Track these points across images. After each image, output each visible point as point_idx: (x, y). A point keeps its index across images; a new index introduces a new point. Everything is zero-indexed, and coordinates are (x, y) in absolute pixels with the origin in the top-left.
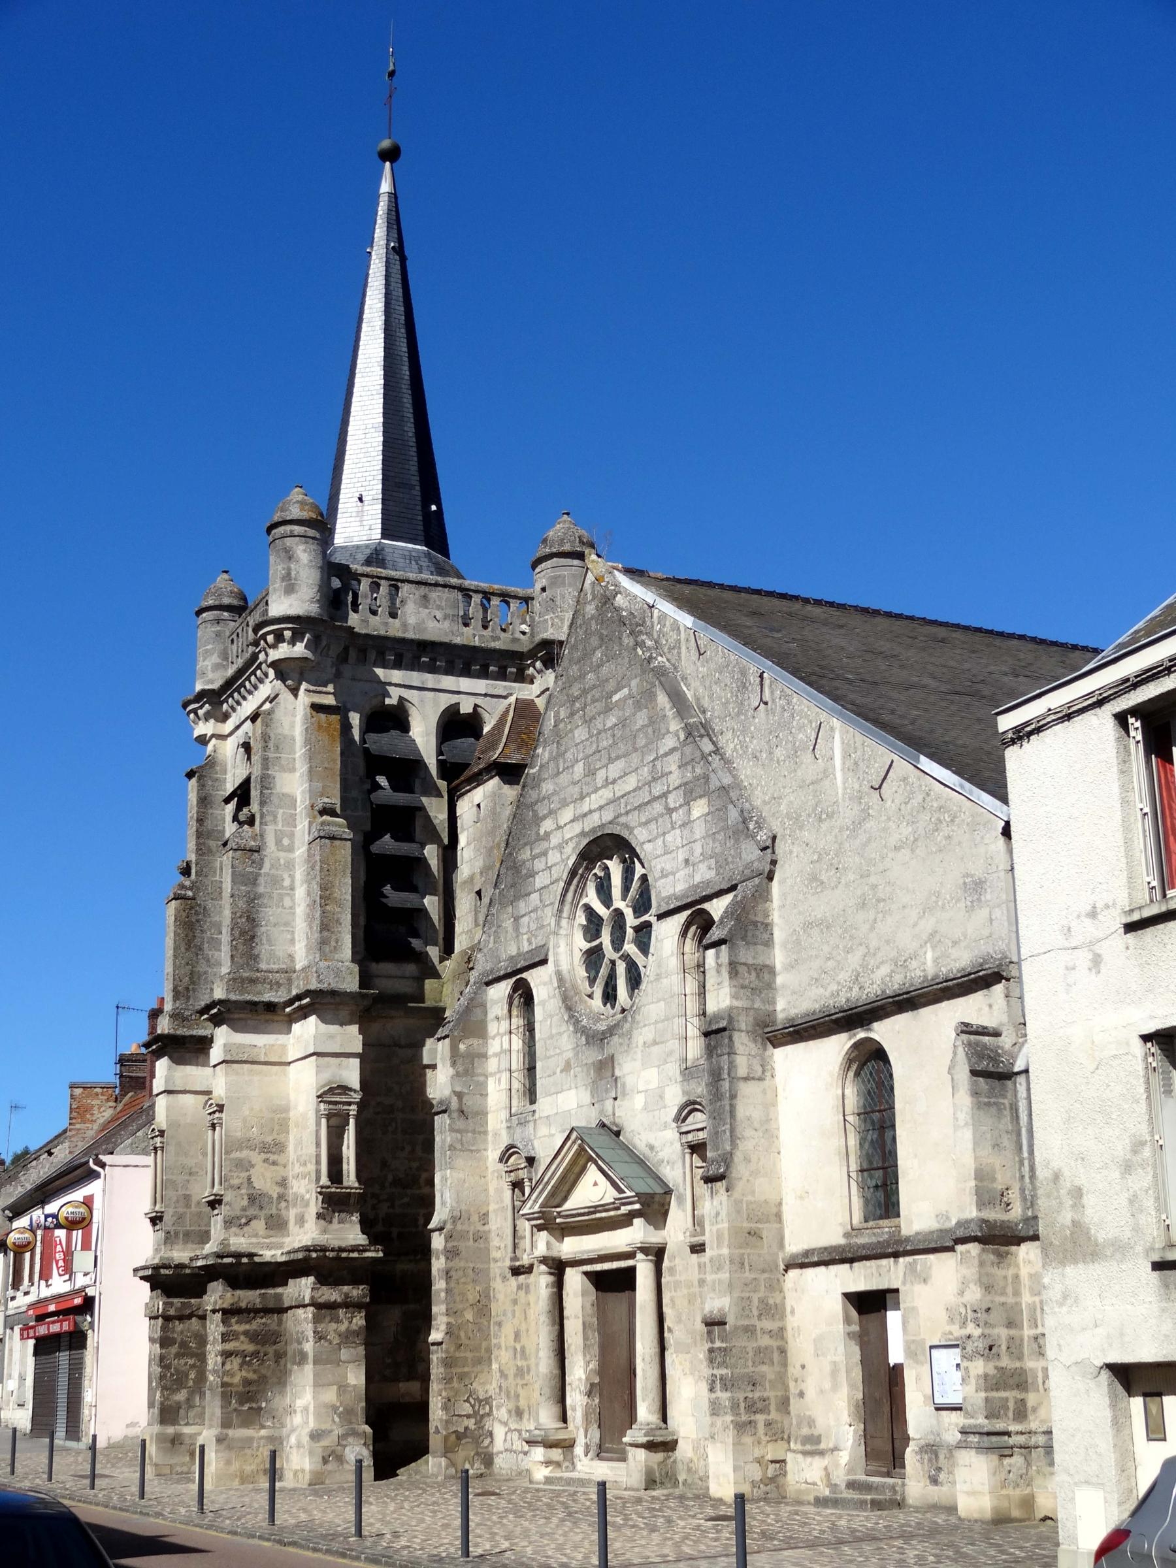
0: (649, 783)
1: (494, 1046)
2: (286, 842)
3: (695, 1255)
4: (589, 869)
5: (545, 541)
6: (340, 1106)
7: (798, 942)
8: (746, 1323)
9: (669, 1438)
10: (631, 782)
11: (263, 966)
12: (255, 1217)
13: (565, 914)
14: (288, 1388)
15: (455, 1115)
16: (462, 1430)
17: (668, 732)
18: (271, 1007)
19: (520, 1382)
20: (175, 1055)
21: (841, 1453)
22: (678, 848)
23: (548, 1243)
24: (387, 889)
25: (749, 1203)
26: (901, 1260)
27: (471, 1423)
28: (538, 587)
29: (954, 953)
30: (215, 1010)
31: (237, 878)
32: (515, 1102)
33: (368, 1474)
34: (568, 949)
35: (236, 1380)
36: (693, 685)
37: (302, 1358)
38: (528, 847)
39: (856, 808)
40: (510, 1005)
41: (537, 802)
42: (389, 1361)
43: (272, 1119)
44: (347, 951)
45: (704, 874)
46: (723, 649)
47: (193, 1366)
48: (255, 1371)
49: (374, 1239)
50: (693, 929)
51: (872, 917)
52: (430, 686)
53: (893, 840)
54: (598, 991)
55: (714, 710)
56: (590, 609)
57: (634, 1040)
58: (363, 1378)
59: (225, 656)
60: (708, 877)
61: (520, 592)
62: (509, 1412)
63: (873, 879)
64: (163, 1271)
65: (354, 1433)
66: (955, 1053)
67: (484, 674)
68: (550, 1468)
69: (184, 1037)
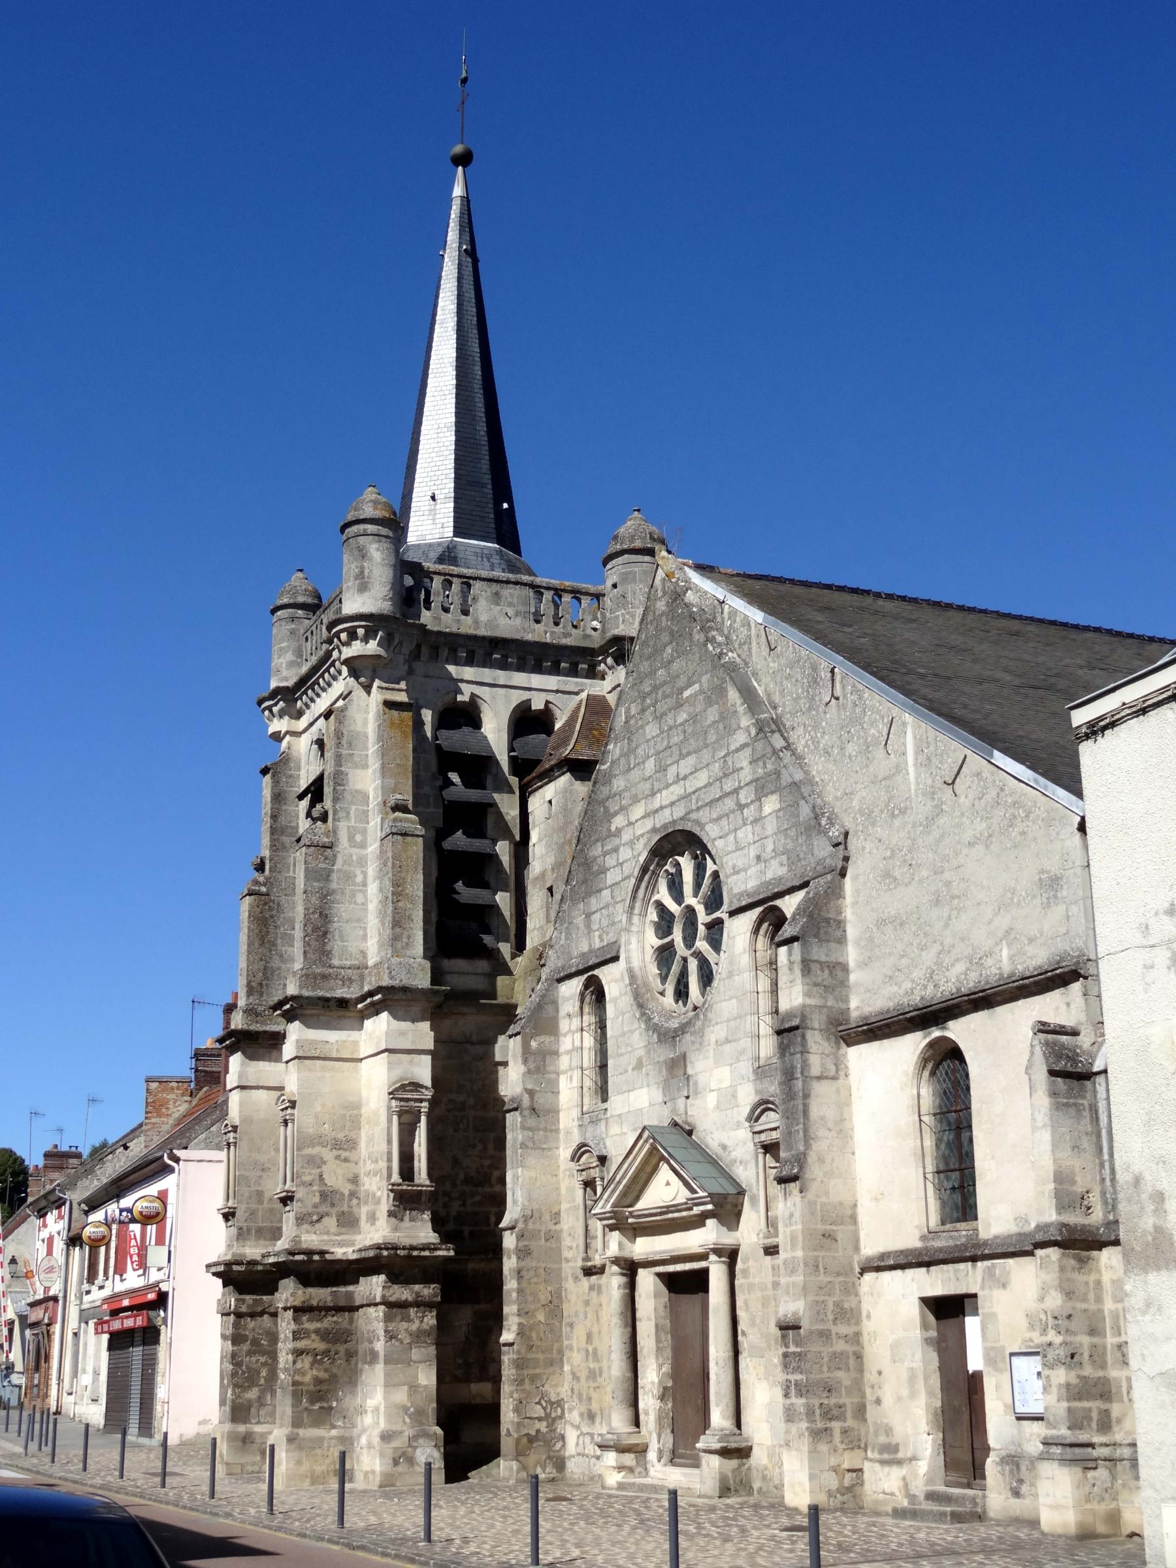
0: (720, 779)
1: (566, 1043)
2: (358, 838)
3: (769, 1257)
4: (660, 865)
5: (616, 537)
6: (412, 1103)
7: (871, 939)
8: (821, 1327)
9: (744, 1445)
10: (702, 778)
11: (336, 962)
12: (327, 1214)
13: (636, 911)
14: (359, 1388)
15: (526, 1113)
16: (533, 1433)
17: (739, 728)
18: (343, 1003)
20: (249, 1051)
21: (920, 1463)
22: (749, 844)
23: (620, 1244)
24: (459, 885)
25: (823, 1204)
26: (979, 1264)
27: (543, 1426)
28: (609, 583)
29: (1030, 950)
30: (288, 1006)
31: (310, 874)
32: (586, 1100)
33: (439, 1477)
34: (640, 945)
35: (307, 1379)
36: (764, 680)
37: (373, 1357)
38: (599, 844)
39: (930, 804)
40: (582, 1001)
42: (460, 1361)
43: (344, 1116)
44: (418, 948)
45: (777, 870)
46: (794, 644)
47: (264, 1364)
48: (326, 1370)
49: (446, 1237)
50: (765, 925)
51: (946, 914)
52: (501, 682)
53: (967, 836)
54: (670, 988)
55: (785, 706)
56: (661, 606)
57: (706, 1038)
58: (434, 1378)
59: (299, 653)
60: (780, 873)
61: (592, 588)
62: (581, 1415)
63: (947, 876)
64: (235, 1268)
65: (425, 1435)
66: (1032, 1053)
67: (555, 670)
68: (622, 1474)
69: (258, 1033)
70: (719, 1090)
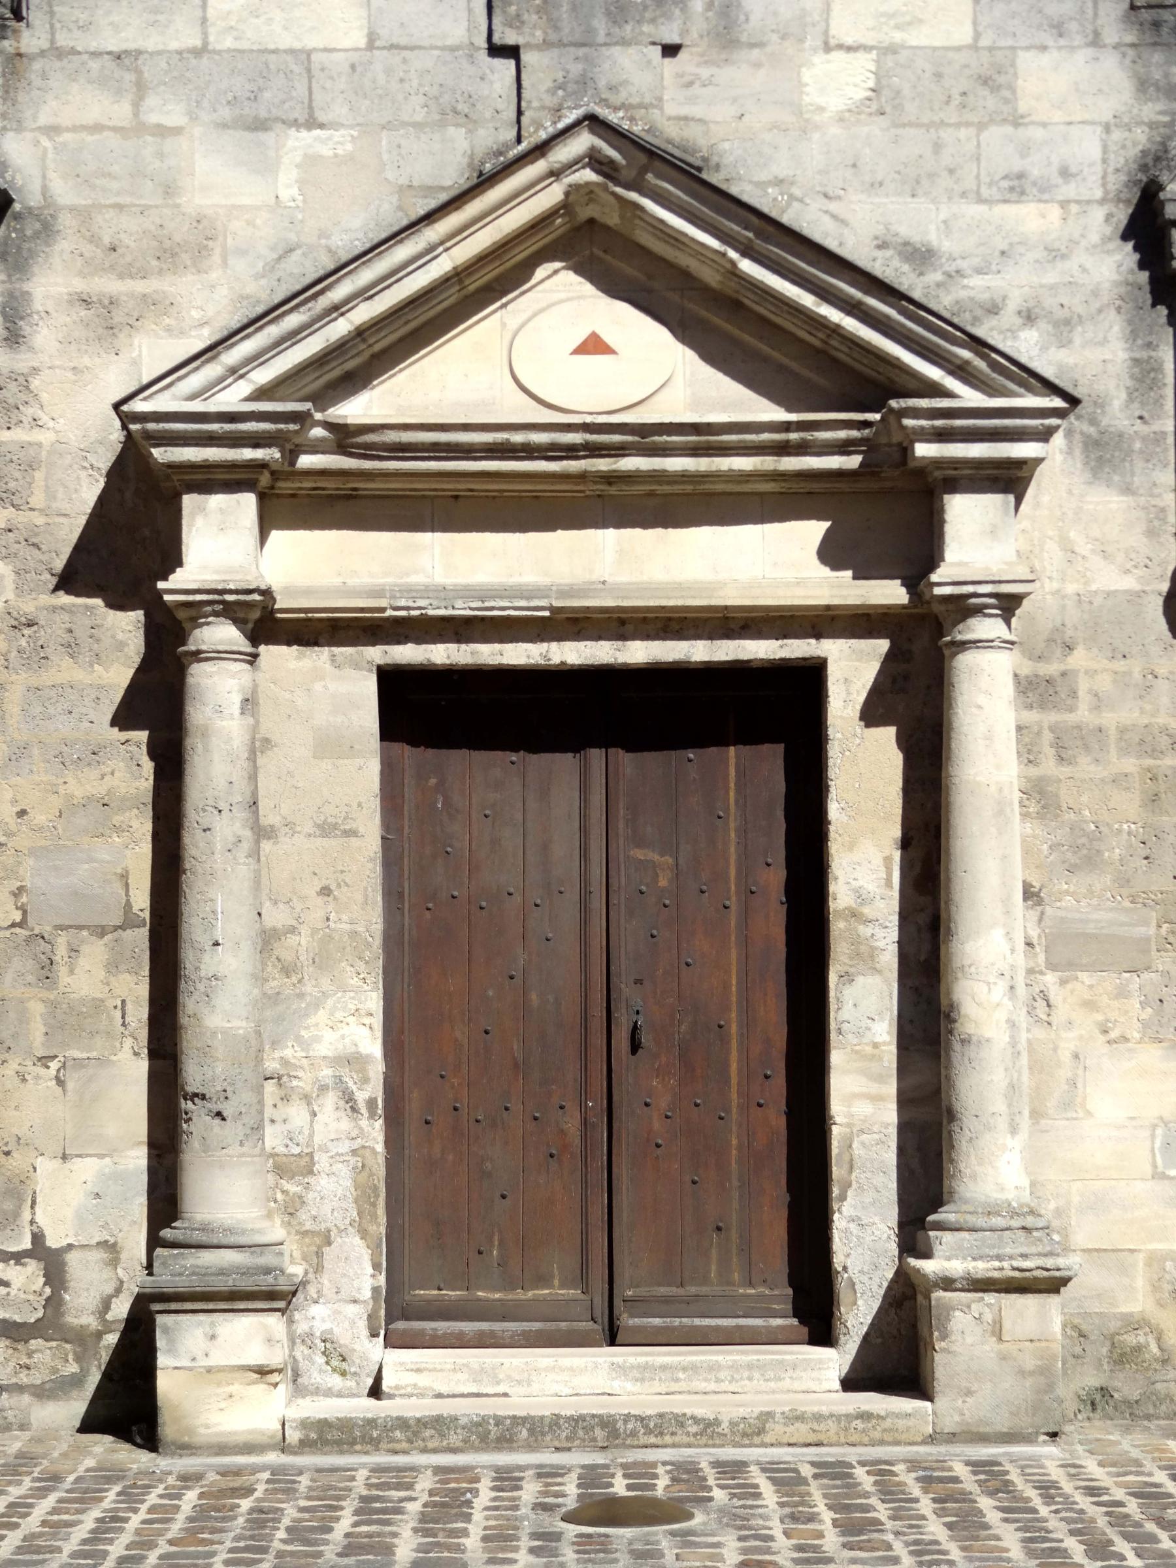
70: (892, 50)
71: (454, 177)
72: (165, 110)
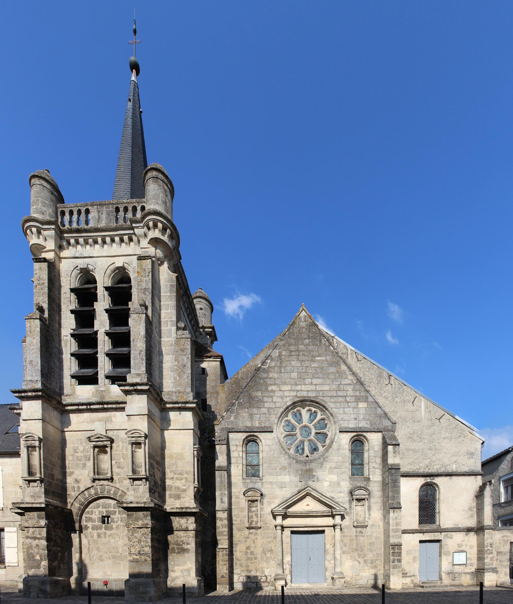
10: (326, 388)
17: (347, 378)
19: (249, 561)
22: (351, 414)
26: (443, 533)
39: (429, 422)
41: (266, 378)
45: (363, 424)
51: (434, 452)
71: (296, 492)
72: (274, 486)
